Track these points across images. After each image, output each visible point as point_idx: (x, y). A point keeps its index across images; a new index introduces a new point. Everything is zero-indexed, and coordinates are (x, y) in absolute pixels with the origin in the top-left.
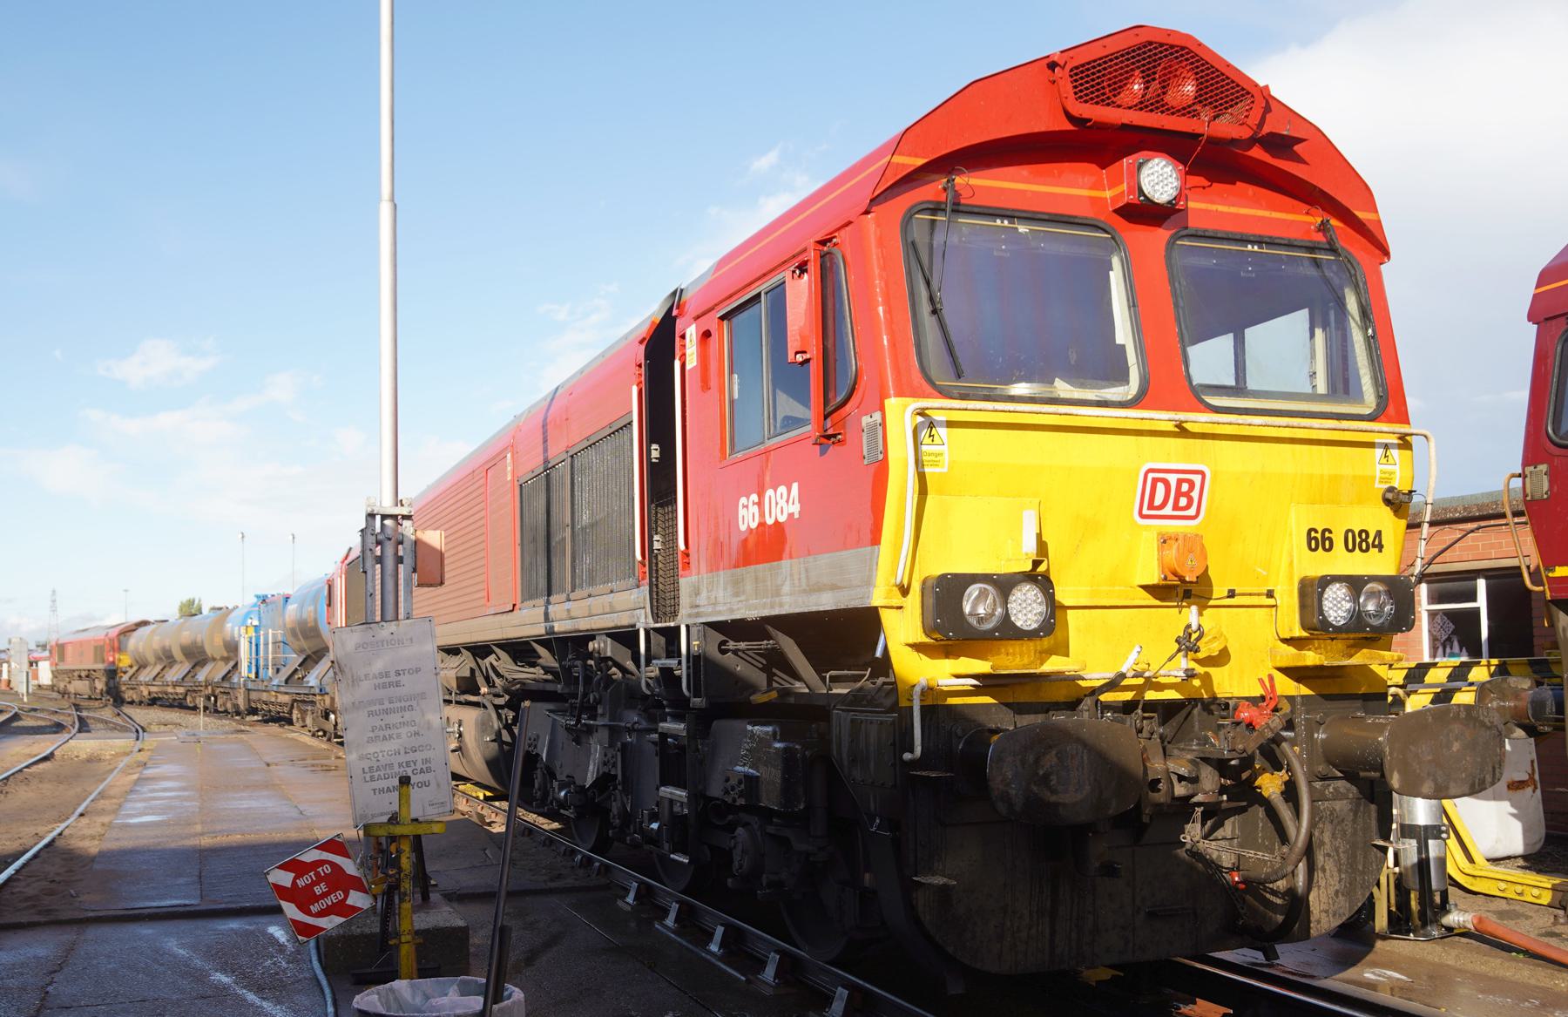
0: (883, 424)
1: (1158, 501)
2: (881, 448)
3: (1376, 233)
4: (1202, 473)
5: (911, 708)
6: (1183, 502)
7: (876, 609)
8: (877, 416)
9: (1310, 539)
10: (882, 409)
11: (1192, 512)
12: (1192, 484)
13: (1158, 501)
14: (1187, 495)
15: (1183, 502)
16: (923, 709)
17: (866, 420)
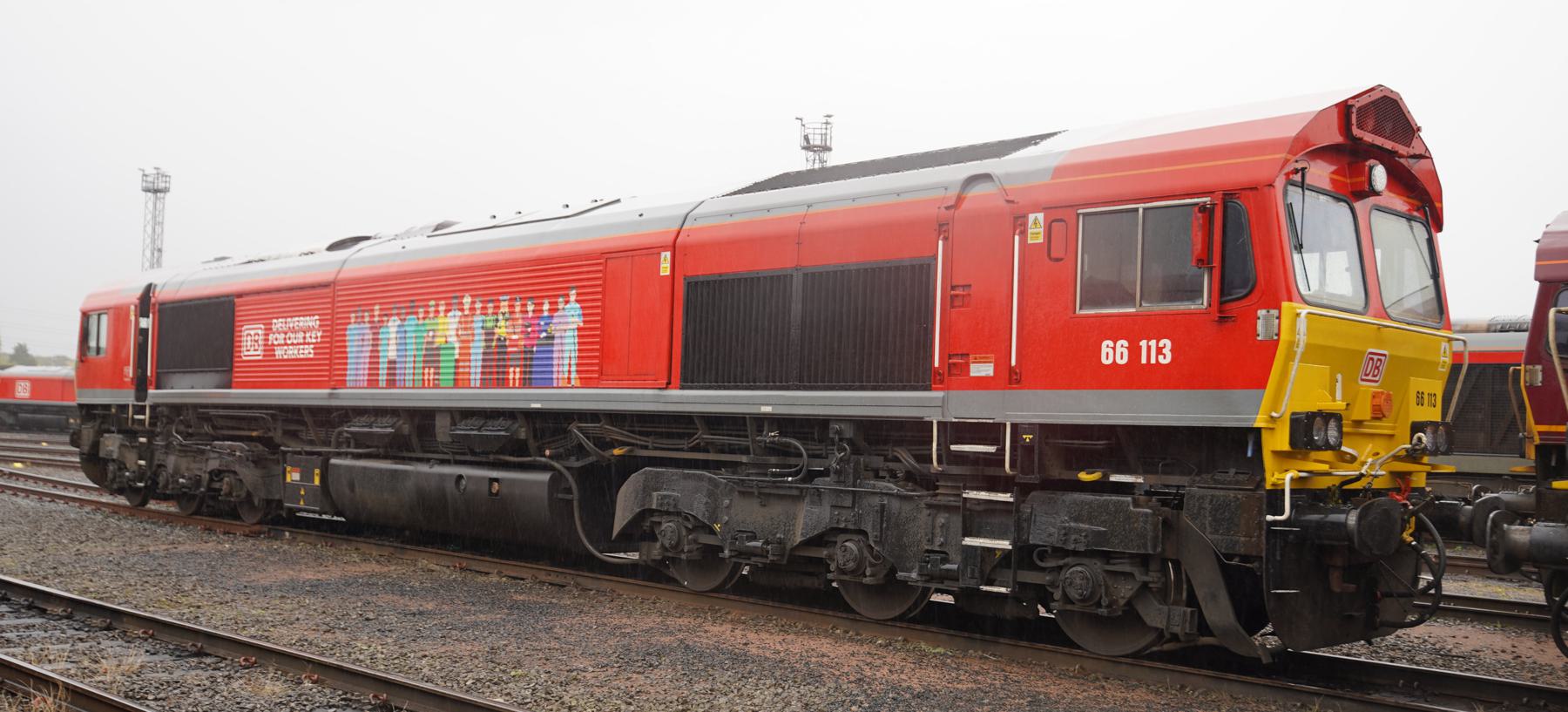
0: (1279, 318)
1: (1368, 372)
2: (1276, 331)
3: (1439, 212)
4: (1385, 355)
5: (1283, 491)
6: (1376, 371)
7: (1259, 429)
8: (1275, 312)
9: (1418, 397)
10: (1279, 308)
11: (1377, 379)
12: (1381, 360)
13: (1368, 372)
14: (1377, 368)
15: (1376, 371)
16: (1292, 491)
17: (1262, 313)
